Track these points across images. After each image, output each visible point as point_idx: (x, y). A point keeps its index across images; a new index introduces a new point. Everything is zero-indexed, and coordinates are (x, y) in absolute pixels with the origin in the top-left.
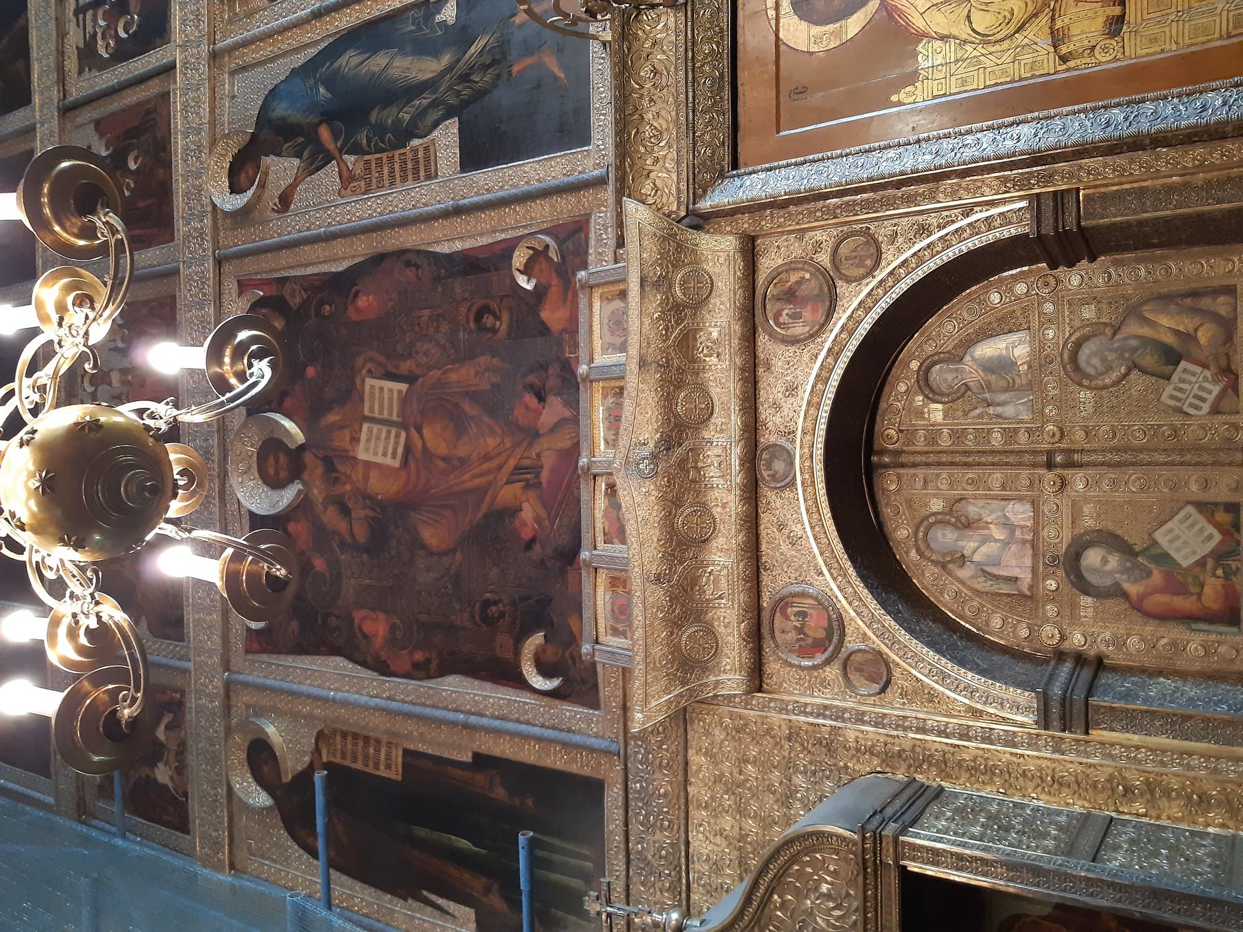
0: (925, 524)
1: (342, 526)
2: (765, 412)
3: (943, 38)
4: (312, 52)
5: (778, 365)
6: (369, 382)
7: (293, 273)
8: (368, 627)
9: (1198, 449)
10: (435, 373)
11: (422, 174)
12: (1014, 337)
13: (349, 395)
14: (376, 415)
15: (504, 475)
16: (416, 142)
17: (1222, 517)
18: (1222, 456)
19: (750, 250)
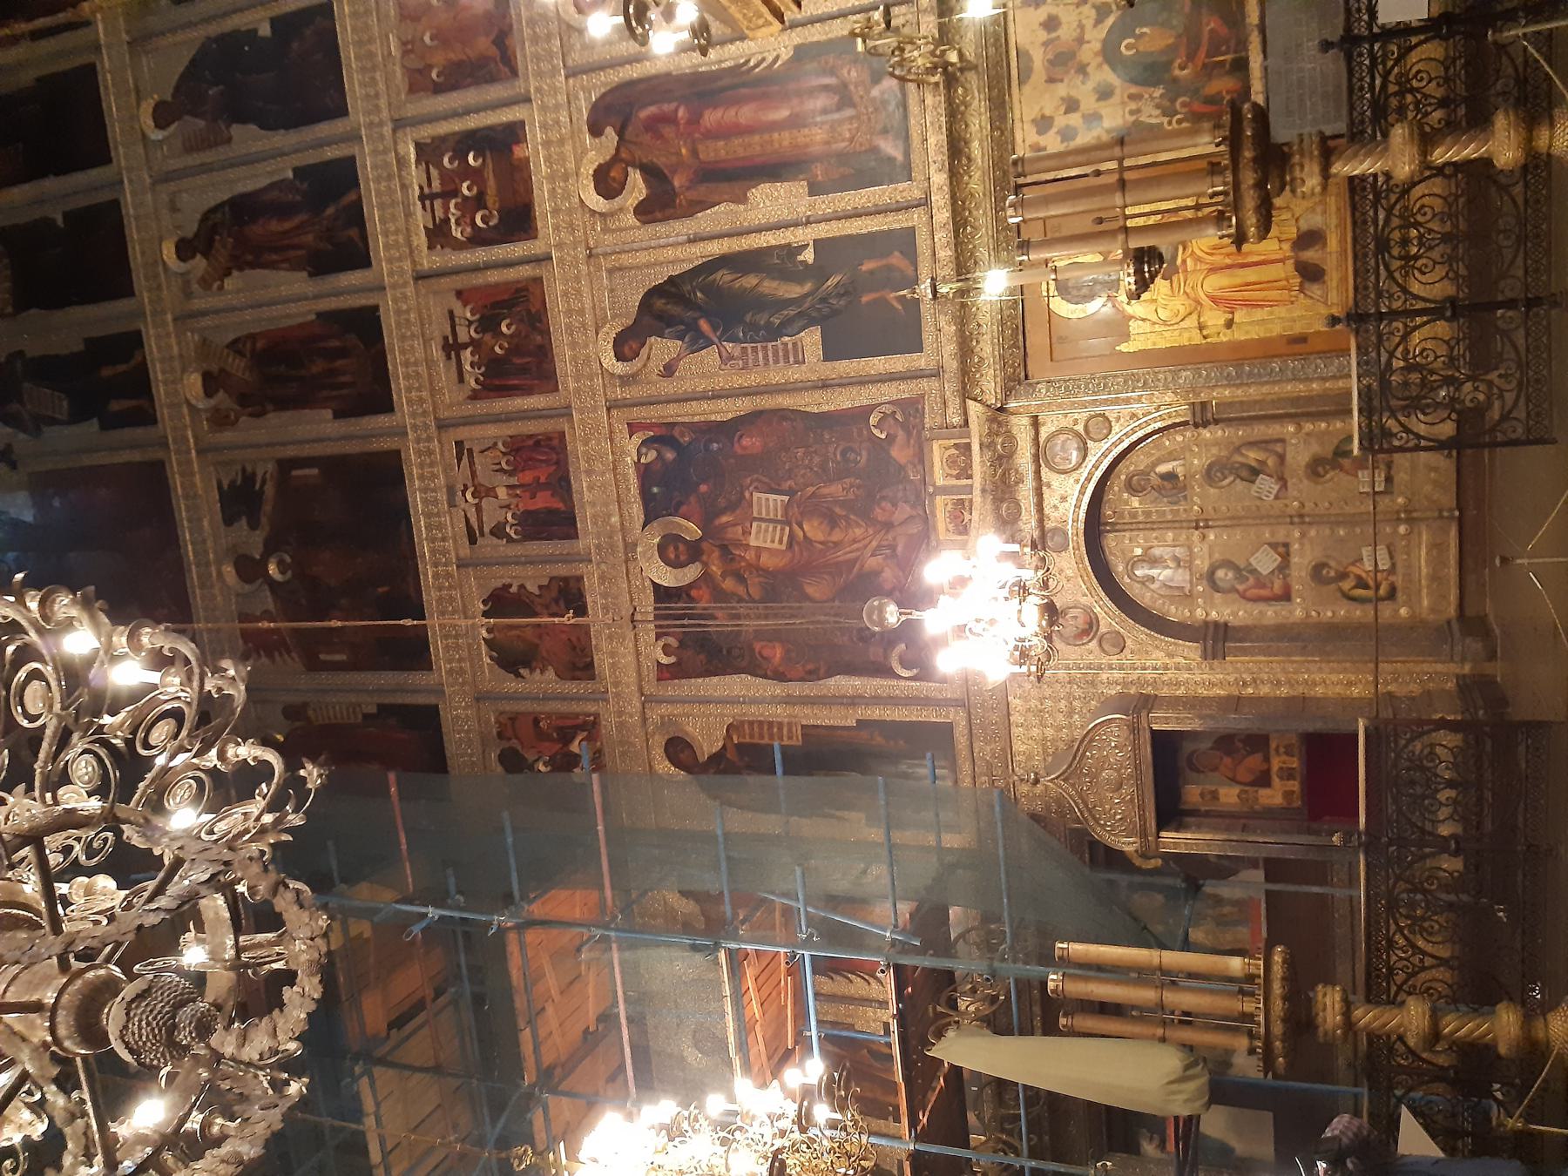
0: (1133, 563)
1: (741, 590)
2: (1047, 511)
3: (1143, 320)
4: (688, 266)
5: (1055, 484)
6: (756, 495)
7: (680, 419)
8: (766, 653)
9: (1269, 516)
10: (811, 490)
11: (792, 359)
12: (1175, 463)
13: (739, 503)
14: (764, 516)
15: (868, 552)
16: (787, 339)
17: (1281, 549)
18: (1280, 520)
19: (1036, 423)
